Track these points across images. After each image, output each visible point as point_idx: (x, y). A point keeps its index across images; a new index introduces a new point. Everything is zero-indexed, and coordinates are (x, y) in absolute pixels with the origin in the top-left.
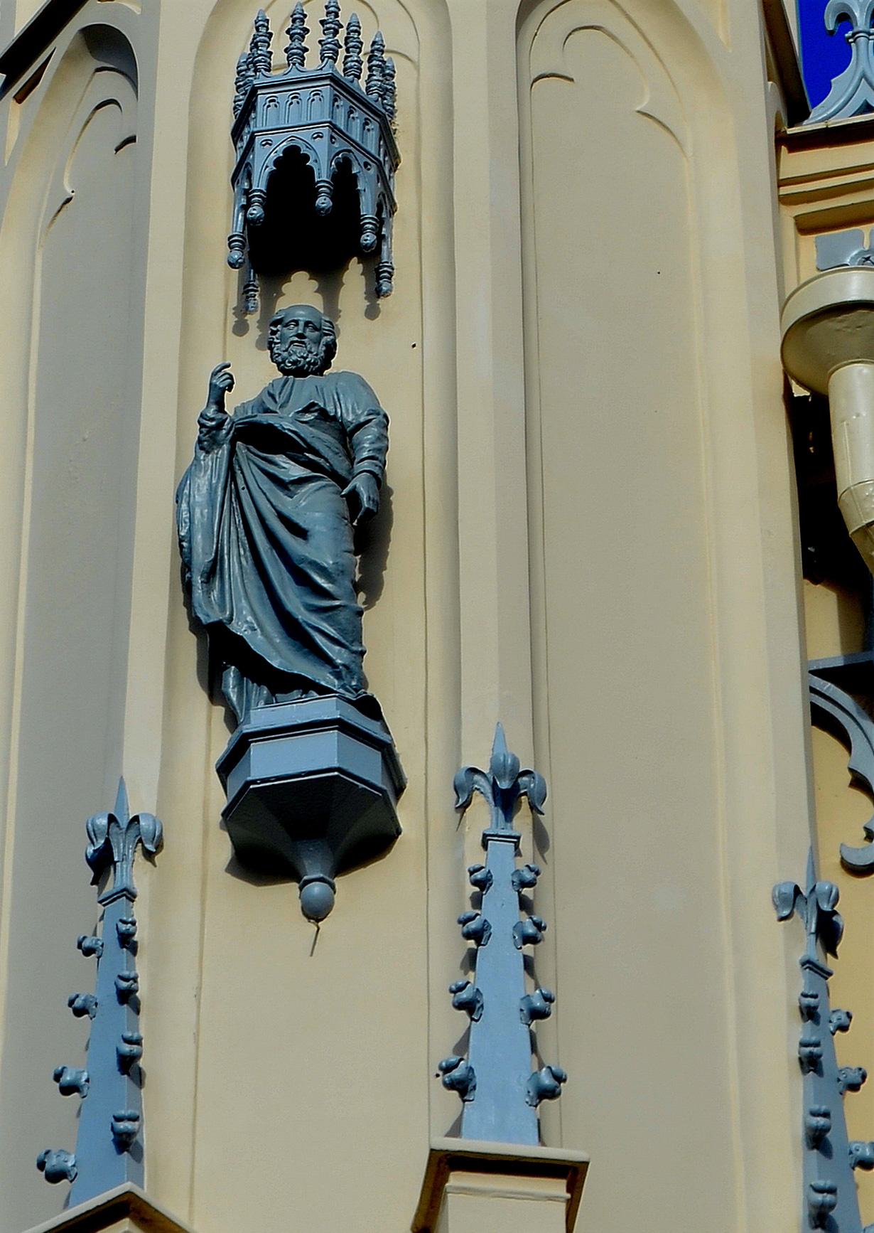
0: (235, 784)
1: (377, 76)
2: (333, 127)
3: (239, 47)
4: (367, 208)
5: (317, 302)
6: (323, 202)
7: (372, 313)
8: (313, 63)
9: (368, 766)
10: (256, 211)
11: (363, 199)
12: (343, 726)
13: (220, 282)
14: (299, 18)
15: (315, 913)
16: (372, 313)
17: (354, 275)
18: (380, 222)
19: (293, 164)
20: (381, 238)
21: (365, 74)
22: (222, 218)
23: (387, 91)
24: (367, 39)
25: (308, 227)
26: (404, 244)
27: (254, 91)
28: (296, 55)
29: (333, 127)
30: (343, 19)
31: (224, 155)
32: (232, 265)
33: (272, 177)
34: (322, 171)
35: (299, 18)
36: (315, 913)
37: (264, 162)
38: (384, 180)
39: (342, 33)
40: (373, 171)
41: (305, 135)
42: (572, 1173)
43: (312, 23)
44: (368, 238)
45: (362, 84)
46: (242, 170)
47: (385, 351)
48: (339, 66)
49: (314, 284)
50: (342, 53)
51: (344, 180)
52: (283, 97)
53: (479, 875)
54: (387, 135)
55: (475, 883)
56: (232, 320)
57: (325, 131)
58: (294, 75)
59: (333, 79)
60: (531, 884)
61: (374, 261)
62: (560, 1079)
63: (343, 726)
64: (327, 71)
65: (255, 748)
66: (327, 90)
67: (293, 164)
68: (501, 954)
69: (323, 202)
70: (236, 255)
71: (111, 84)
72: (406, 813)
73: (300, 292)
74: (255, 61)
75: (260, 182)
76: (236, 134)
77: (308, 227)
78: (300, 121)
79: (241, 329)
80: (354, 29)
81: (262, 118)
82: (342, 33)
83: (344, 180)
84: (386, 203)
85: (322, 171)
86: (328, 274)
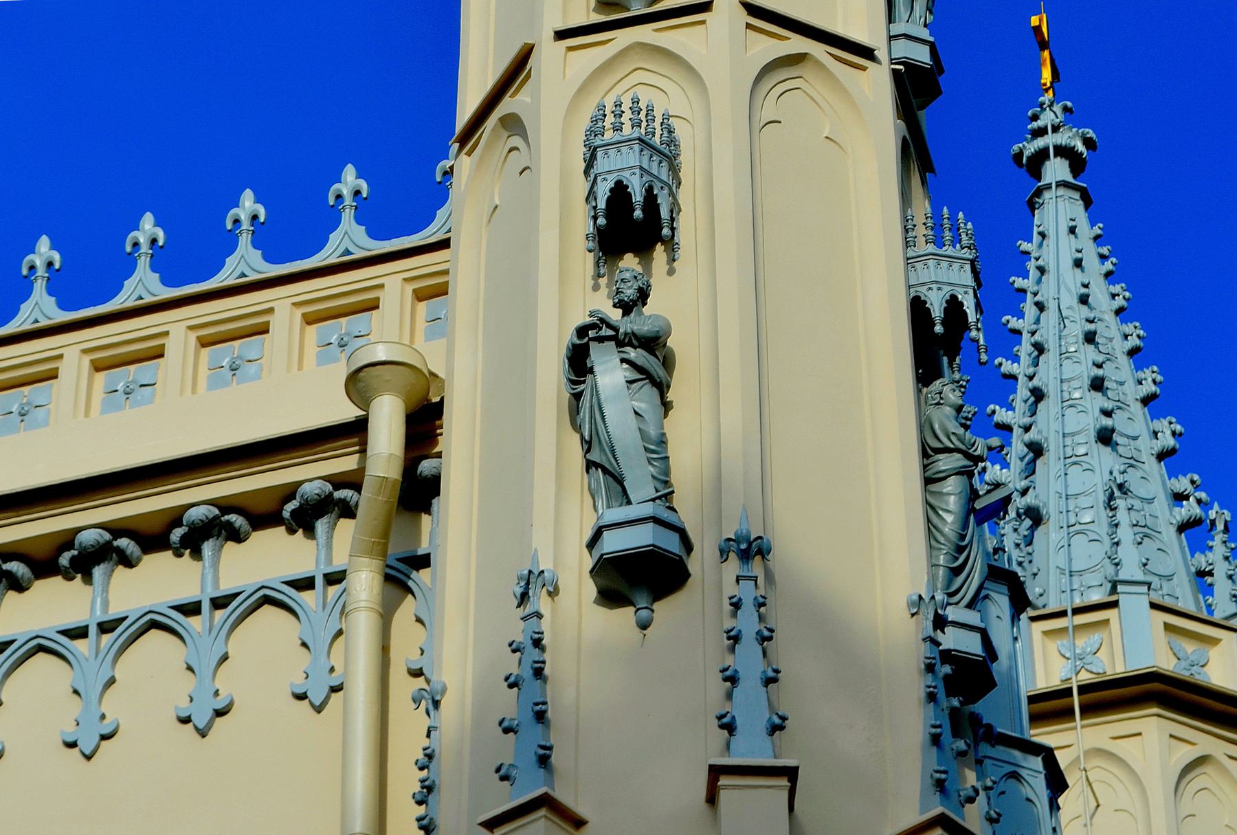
0: (596, 554)
1: (666, 134)
2: (641, 168)
3: (584, 123)
4: (664, 213)
5: (639, 269)
6: (638, 214)
7: (671, 272)
8: (627, 130)
9: (671, 543)
10: (602, 221)
11: (662, 210)
12: (656, 520)
13: (584, 260)
14: (618, 105)
15: (644, 626)
16: (671, 272)
17: (659, 251)
18: (672, 219)
19: (620, 192)
20: (673, 229)
21: (658, 132)
22: (582, 225)
23: (672, 142)
24: (658, 114)
25: (630, 228)
26: (688, 230)
27: (595, 148)
28: (618, 128)
29: (641, 168)
30: (643, 105)
31: (582, 186)
32: (590, 251)
33: (609, 200)
34: (638, 197)
35: (618, 105)
36: (644, 626)
37: (604, 190)
38: (672, 194)
39: (642, 115)
40: (666, 191)
41: (627, 174)
42: (791, 774)
43: (625, 107)
44: (666, 231)
45: (657, 139)
46: (591, 195)
47: (678, 295)
48: (643, 131)
49: (637, 260)
50: (644, 124)
51: (650, 200)
52: (612, 152)
53: (734, 600)
54: (674, 169)
55: (731, 604)
56: (590, 283)
57: (637, 171)
58: (617, 138)
59: (640, 139)
60: (763, 604)
61: (671, 245)
62: (784, 719)
63: (656, 520)
64: (636, 135)
65: (606, 534)
66: (637, 147)
67: (620, 192)
68: (749, 645)
69: (638, 214)
70: (591, 244)
71: (516, 141)
72: (693, 564)
73: (630, 262)
74: (592, 132)
75: (602, 205)
76: (587, 172)
77: (630, 228)
78: (625, 165)
79: (596, 288)
80: (650, 109)
81: (601, 165)
82: (642, 115)
83: (650, 200)
84: (675, 209)
85: (638, 197)
86: (643, 249)
